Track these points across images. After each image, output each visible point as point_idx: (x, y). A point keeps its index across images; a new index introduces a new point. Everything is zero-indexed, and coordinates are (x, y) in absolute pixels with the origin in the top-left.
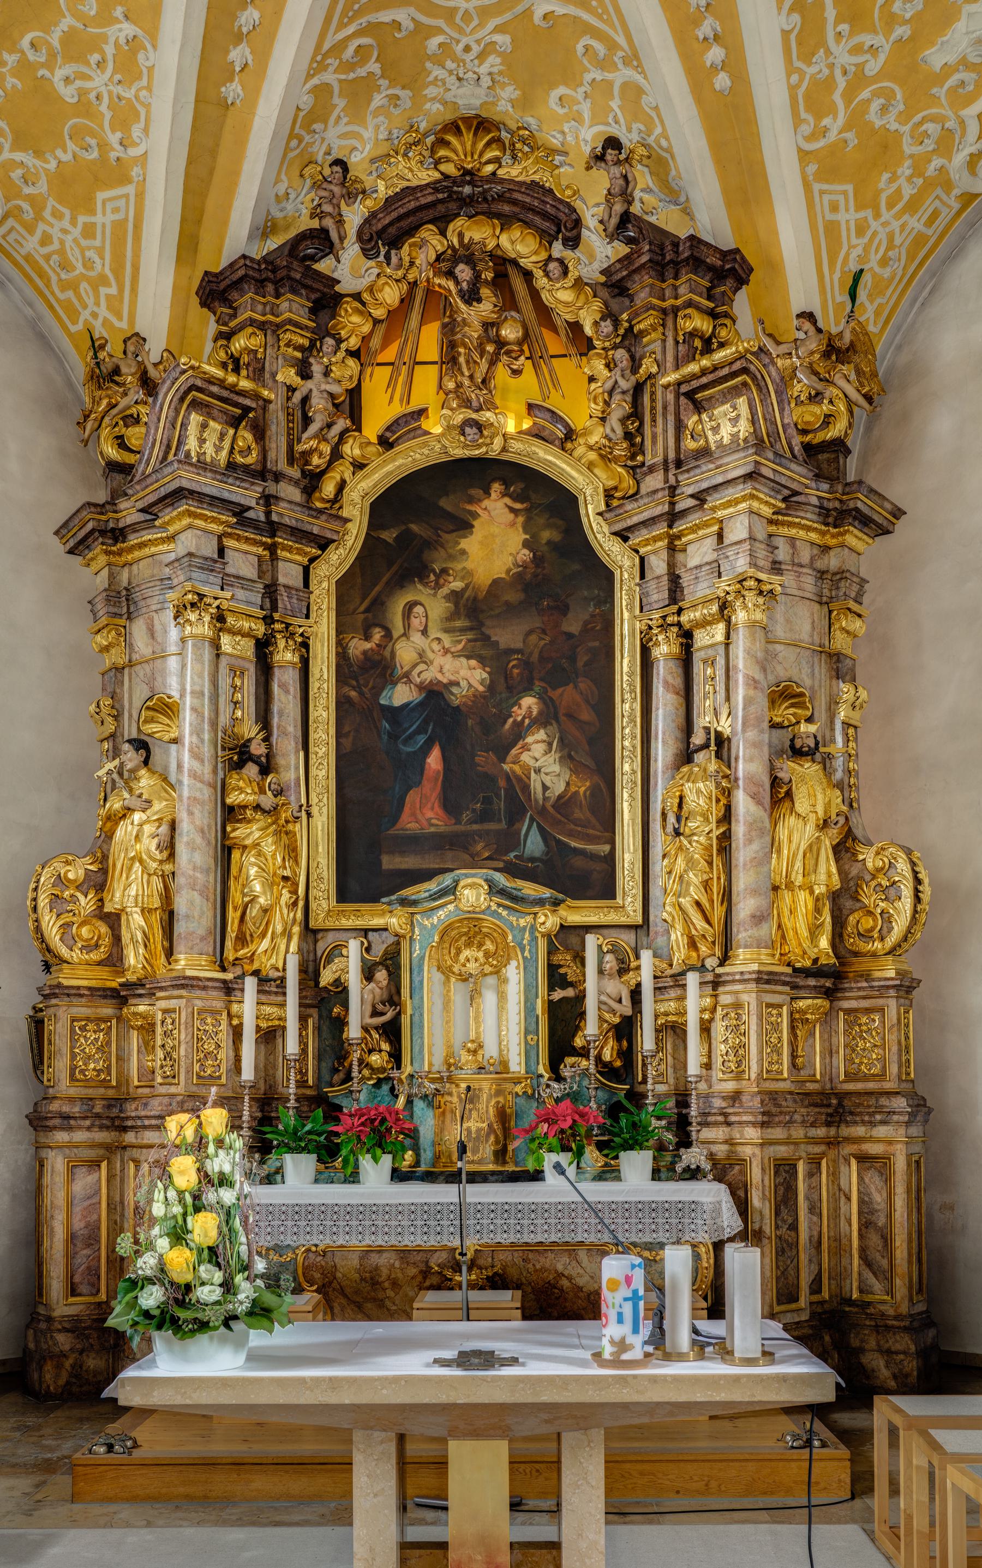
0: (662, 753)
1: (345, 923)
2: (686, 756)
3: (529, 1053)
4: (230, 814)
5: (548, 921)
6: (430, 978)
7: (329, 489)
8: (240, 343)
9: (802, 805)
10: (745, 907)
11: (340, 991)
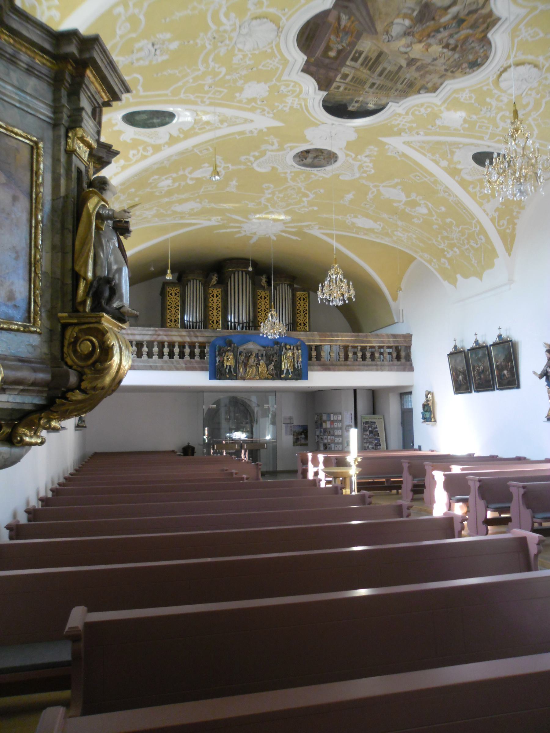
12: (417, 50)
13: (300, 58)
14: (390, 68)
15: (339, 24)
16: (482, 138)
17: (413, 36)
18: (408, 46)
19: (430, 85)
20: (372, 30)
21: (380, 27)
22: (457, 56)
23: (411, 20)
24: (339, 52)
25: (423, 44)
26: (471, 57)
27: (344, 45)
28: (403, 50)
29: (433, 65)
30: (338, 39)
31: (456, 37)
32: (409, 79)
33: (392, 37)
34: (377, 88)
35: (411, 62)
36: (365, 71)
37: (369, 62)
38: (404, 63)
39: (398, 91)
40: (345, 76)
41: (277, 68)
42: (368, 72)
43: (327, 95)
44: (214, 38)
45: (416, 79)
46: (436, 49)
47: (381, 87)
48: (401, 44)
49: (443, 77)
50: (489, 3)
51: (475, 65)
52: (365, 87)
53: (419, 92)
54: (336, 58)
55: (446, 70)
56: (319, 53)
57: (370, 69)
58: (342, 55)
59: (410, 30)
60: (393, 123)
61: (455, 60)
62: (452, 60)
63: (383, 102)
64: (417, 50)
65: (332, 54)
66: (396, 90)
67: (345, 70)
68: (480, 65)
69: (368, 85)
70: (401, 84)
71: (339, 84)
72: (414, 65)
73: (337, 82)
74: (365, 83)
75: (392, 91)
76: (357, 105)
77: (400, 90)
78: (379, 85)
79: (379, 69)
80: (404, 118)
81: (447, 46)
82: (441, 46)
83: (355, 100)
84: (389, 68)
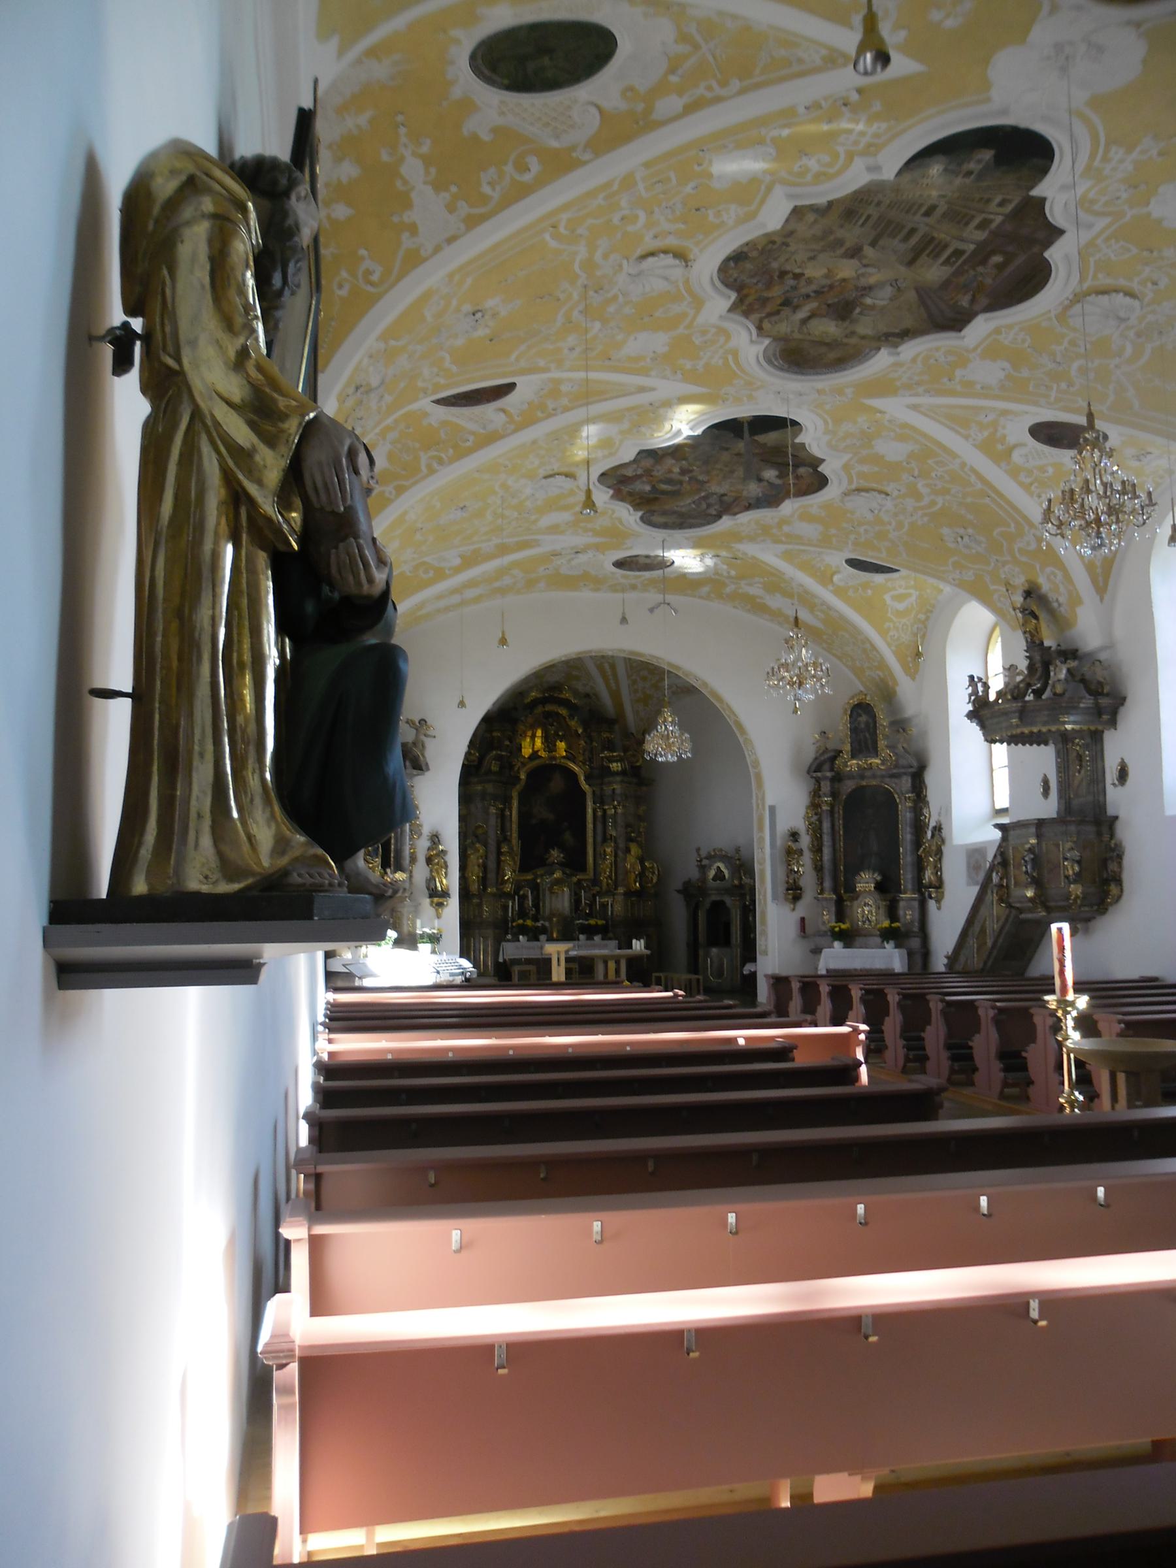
0: (599, 839)
1: (524, 878)
2: (605, 840)
3: (571, 910)
4: (499, 853)
5: (575, 879)
6: (547, 892)
7: (516, 769)
8: (496, 734)
9: (632, 853)
10: (621, 877)
11: (525, 897)
12: (847, 270)
13: (1055, 254)
14: (896, 243)
15: (974, 296)
16: (647, 165)
17: (857, 288)
18: (863, 275)
19: (811, 217)
20: (923, 294)
21: (912, 295)
22: (775, 265)
23: (862, 304)
24: (984, 262)
25: (838, 277)
26: (748, 266)
27: (972, 273)
28: (870, 270)
29: (813, 250)
30: (980, 279)
31: (787, 288)
32: (855, 224)
33: (891, 285)
34: (921, 205)
35: (854, 253)
36: (942, 236)
37: (932, 251)
38: (868, 251)
39: (876, 200)
40: (982, 226)
41: (1108, 239)
42: (936, 235)
43: (1032, 188)
44: (1161, 333)
45: (842, 226)
46: (815, 272)
47: (911, 208)
48: (873, 279)
49: (787, 233)
50: (754, 325)
51: (737, 257)
52: (946, 207)
53: (830, 204)
54: (993, 252)
55: (787, 245)
56: (1020, 260)
57: (933, 238)
58: (981, 255)
59: (863, 292)
60: (884, 125)
61: (775, 259)
62: (782, 259)
63: (907, 177)
64: (847, 270)
65: (997, 259)
66: (879, 204)
67: (981, 236)
68: (728, 259)
69: (939, 212)
70: (869, 217)
71: (1000, 210)
72: (849, 249)
73: (1002, 215)
74: (944, 215)
75: (888, 202)
76: (971, 165)
77: (870, 204)
78: (915, 214)
79: (914, 240)
80: (856, 143)
81: (797, 276)
82: (806, 276)
83: (972, 177)
84: (896, 242)
